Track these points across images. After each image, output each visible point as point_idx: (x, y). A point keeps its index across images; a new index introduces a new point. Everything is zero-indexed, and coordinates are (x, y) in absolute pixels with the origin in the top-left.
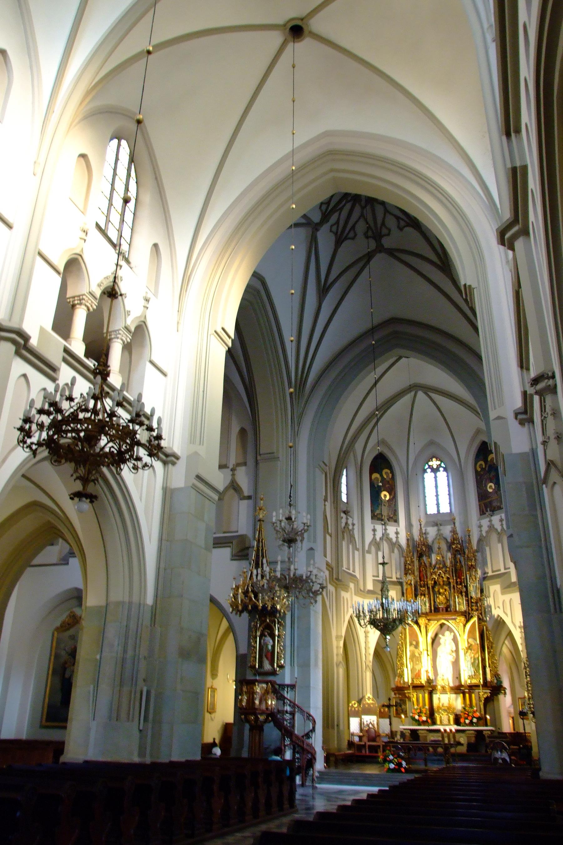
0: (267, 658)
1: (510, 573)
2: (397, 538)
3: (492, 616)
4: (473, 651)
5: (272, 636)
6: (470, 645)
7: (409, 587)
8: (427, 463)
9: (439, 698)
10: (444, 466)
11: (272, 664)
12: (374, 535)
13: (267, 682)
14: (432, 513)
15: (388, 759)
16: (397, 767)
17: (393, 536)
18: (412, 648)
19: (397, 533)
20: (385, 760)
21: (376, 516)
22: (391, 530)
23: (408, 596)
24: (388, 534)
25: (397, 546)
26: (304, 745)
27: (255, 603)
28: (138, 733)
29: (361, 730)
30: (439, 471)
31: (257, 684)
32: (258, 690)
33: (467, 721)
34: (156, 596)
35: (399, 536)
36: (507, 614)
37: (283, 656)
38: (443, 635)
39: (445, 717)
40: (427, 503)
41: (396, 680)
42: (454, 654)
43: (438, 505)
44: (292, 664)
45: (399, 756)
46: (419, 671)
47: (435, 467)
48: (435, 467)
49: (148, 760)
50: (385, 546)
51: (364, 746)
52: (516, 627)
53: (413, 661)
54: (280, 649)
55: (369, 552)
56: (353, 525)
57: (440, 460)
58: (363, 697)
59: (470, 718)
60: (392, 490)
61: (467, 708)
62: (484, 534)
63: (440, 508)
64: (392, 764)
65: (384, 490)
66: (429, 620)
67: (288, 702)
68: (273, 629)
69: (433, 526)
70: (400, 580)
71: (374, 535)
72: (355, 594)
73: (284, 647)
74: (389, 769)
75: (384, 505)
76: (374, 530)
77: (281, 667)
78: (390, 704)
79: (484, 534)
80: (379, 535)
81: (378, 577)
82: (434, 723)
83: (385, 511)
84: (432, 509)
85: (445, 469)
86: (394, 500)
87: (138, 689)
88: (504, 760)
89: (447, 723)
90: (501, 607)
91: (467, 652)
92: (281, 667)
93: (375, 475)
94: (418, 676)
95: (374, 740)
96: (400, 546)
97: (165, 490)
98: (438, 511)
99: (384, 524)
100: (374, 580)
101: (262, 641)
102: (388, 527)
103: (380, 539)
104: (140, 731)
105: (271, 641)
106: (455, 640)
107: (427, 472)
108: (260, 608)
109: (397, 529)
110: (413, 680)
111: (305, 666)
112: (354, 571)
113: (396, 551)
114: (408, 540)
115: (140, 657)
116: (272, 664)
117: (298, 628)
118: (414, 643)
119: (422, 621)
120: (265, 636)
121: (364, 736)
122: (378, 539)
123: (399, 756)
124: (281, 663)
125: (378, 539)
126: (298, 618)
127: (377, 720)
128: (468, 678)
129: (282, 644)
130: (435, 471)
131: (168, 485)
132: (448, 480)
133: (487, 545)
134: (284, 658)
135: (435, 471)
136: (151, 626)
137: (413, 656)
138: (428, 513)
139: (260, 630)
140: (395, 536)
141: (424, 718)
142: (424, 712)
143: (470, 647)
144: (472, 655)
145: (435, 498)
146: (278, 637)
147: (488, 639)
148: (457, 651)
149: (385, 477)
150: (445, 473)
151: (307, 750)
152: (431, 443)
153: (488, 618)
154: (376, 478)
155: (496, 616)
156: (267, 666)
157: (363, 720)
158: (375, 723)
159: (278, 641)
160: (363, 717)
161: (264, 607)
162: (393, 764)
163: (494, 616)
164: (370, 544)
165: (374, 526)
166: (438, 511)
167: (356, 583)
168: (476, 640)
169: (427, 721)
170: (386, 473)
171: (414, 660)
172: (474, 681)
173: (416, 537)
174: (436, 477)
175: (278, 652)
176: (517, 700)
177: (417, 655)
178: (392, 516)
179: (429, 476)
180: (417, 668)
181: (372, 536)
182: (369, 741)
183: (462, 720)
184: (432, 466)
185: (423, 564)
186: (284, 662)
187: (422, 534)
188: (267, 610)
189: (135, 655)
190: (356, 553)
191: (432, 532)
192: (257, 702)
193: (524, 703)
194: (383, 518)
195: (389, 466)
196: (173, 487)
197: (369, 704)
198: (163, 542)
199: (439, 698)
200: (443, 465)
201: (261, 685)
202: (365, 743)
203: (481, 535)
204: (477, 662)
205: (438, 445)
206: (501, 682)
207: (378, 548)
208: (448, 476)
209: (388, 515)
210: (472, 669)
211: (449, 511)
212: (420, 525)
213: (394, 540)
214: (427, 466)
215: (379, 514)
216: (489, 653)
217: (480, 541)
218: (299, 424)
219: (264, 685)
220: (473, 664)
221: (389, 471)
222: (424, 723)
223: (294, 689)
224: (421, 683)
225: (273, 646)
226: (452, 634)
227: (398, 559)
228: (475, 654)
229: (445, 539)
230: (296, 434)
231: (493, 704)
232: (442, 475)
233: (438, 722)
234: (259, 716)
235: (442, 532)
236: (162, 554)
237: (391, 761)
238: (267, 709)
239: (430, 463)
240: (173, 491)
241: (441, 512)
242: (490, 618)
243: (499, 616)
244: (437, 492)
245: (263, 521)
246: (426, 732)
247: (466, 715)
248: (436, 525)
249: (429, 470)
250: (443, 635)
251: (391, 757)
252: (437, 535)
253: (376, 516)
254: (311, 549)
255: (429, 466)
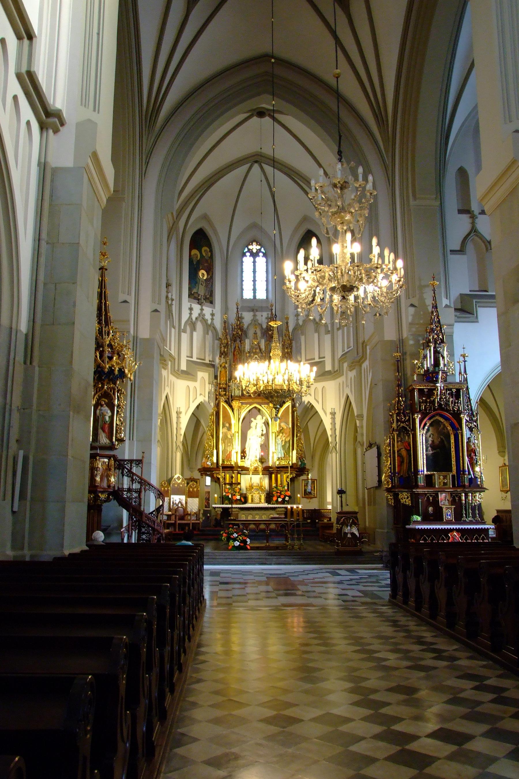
0: (104, 431)
1: (325, 363)
2: (212, 319)
3: (301, 403)
4: (284, 435)
5: (111, 406)
6: (281, 429)
7: (223, 369)
8: (247, 247)
9: (251, 478)
10: (264, 252)
11: (110, 438)
12: (191, 314)
13: (109, 457)
14: (248, 298)
15: (232, 536)
16: (242, 544)
17: (208, 317)
18: (225, 430)
19: (213, 315)
20: (229, 539)
21: (193, 294)
22: (207, 311)
23: (222, 379)
24: (204, 315)
25: (212, 328)
26: (154, 525)
27: (100, 364)
28: (9, 516)
29: (170, 510)
30: (259, 256)
31: (98, 458)
32: (100, 466)
33: (280, 500)
34: (33, 320)
35: (214, 317)
36: (318, 402)
37: (123, 429)
38: (255, 419)
39: (256, 496)
40: (244, 287)
41: (204, 461)
42: (263, 437)
43: (254, 290)
44: (131, 438)
45: (244, 534)
46: (230, 452)
47: (255, 251)
48: (255, 251)
49: (27, 554)
50: (199, 326)
51: (174, 525)
52: (326, 414)
53: (224, 443)
54: (120, 420)
55: (185, 331)
56: (172, 300)
57: (260, 245)
58: (172, 477)
59: (282, 497)
60: (210, 270)
61: (279, 488)
62: (301, 323)
63: (257, 294)
64: (236, 542)
65: (202, 269)
66: (242, 403)
67: (138, 479)
68: (111, 396)
69: (249, 311)
70: (213, 363)
71: (191, 314)
72: (171, 373)
73: (125, 418)
74: (234, 546)
75: (201, 284)
76: (191, 309)
77: (121, 441)
78: (232, 482)
79: (301, 323)
80: (195, 314)
81: (192, 357)
82: (246, 502)
83: (201, 290)
84: (248, 294)
85: (265, 255)
86: (211, 280)
87: (11, 453)
88: (353, 534)
89: (258, 502)
90: (313, 394)
91: (278, 436)
92: (121, 441)
93: (195, 252)
94: (228, 457)
95: (182, 518)
96: (214, 328)
97: (43, 166)
98: (255, 296)
99: (200, 303)
100: (187, 360)
101: (98, 411)
102: (204, 307)
103: (196, 319)
104: (13, 512)
105: (109, 411)
106: (267, 424)
107: (246, 256)
108: (106, 370)
109: (212, 311)
110: (223, 461)
111: (146, 441)
112: (170, 349)
113: (210, 333)
114: (225, 322)
115: (13, 407)
116: (110, 438)
117: (138, 398)
118: (227, 425)
119: (236, 404)
120: (102, 406)
121: (173, 514)
122: (194, 319)
123: (244, 534)
124: (120, 436)
125: (194, 319)
126: (139, 387)
127: (186, 499)
128: (277, 460)
129: (123, 415)
130: (254, 255)
131: (50, 159)
132: (267, 266)
133: (303, 334)
134: (125, 431)
135: (254, 255)
136: (25, 363)
137: (225, 437)
138: (245, 297)
139: (95, 397)
140: (210, 317)
141: (238, 497)
142: (238, 491)
143: (281, 431)
144: (284, 439)
145: (252, 283)
146: (117, 408)
147: (297, 425)
148: (266, 436)
149: (204, 254)
150: (264, 259)
151: (157, 530)
152: (254, 226)
153: (297, 405)
154: (195, 254)
155: (306, 403)
156: (103, 439)
157: (172, 500)
158: (184, 502)
159: (118, 411)
160: (172, 496)
161: (111, 371)
162: (238, 542)
163: (304, 402)
164: (186, 323)
165: (191, 305)
166: (255, 296)
167: (173, 361)
168: (289, 425)
169: (240, 500)
170: (205, 251)
171: (226, 441)
172: (283, 463)
173: (232, 320)
174: (254, 262)
175: (117, 424)
176: (301, 482)
177: (229, 436)
178: (208, 296)
179: (248, 260)
180: (229, 449)
181: (189, 315)
182: (180, 519)
183: (275, 499)
184: (252, 250)
185: (237, 348)
186: (125, 436)
187: (239, 318)
188: (114, 374)
189: (5, 404)
190: (173, 330)
191: (247, 317)
192: (98, 479)
193: (307, 484)
194: (200, 297)
195: (209, 245)
196: (54, 166)
197: (180, 484)
198: (43, 244)
199: (251, 478)
200: (263, 250)
201: (103, 460)
202: (175, 521)
203: (297, 324)
204: (288, 445)
205: (261, 229)
206: (305, 464)
207: (193, 328)
208: (267, 262)
209: (205, 296)
210: (282, 452)
211: (265, 298)
212: (237, 308)
213: (209, 322)
214: (246, 250)
215: (197, 293)
216: (297, 436)
217: (294, 329)
218: (148, 163)
219: (106, 460)
220: (283, 447)
221: (208, 250)
222: (237, 501)
223: (140, 465)
224: (231, 464)
225: (112, 418)
226: (264, 418)
227: (211, 342)
228: (288, 436)
229: (261, 325)
230: (143, 175)
231: (294, 483)
232: (261, 261)
233: (250, 501)
234: (100, 494)
235: (257, 318)
236: (42, 260)
237: (235, 540)
238: (109, 486)
239: (250, 247)
240: (55, 171)
241: (257, 297)
242: (299, 405)
243: (309, 402)
244: (254, 277)
245: (106, 270)
246: (238, 509)
247: (279, 494)
248: (253, 310)
249: (248, 254)
250: (255, 419)
251: (235, 535)
252: (252, 320)
253: (193, 294)
254: (156, 311)
255: (250, 251)
